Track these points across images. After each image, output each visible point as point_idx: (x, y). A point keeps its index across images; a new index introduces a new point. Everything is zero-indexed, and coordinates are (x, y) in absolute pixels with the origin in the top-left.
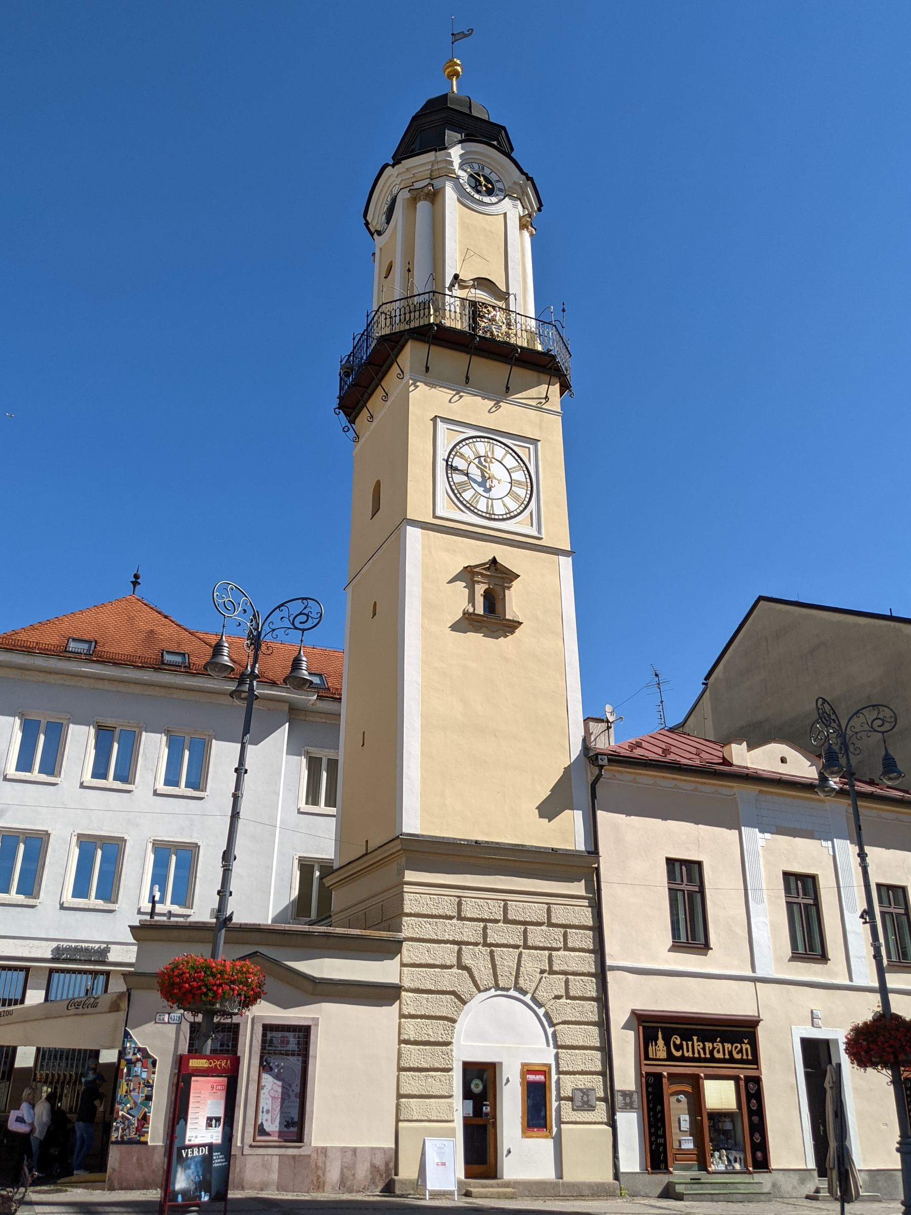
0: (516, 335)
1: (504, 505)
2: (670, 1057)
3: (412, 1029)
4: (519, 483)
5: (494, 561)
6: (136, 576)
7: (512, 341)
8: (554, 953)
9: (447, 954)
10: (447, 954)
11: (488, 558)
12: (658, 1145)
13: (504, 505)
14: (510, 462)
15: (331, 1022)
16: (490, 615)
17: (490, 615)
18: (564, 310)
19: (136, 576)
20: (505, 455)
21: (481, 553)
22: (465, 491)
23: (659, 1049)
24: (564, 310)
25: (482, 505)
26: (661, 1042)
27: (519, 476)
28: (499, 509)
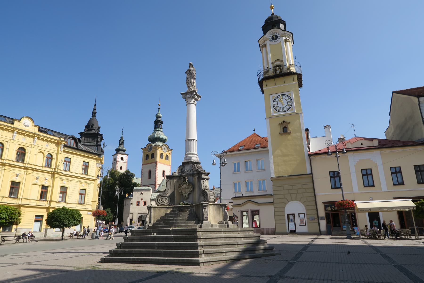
2: (332, 210)
3: (276, 210)
5: (284, 121)
14: (287, 98)
15: (263, 209)
23: (329, 209)
26: (329, 207)
28: (285, 109)
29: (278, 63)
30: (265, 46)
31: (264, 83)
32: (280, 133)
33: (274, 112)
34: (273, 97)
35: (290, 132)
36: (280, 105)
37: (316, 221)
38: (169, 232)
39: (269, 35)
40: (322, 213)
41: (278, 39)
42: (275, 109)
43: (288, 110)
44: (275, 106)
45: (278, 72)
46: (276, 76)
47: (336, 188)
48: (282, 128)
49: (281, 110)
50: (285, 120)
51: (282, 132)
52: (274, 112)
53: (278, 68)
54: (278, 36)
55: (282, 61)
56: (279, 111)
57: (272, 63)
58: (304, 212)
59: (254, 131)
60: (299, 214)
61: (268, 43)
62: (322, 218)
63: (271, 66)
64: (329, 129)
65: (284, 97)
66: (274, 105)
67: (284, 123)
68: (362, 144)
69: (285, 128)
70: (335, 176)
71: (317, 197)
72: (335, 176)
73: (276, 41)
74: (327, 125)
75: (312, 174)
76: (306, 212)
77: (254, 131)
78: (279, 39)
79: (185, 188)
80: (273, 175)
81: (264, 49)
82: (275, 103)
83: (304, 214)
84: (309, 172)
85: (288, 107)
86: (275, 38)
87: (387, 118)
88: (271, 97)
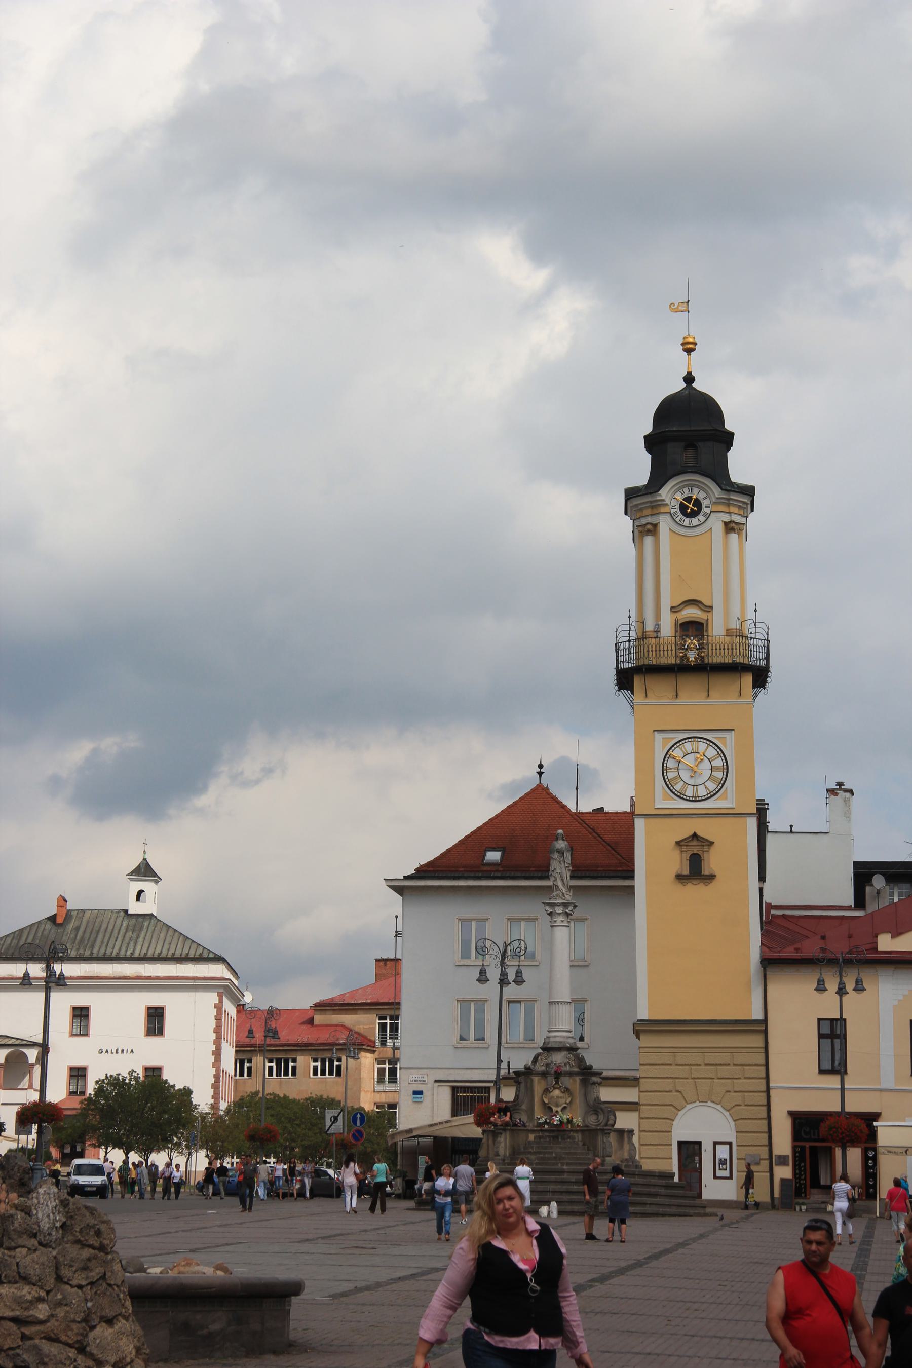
1: (706, 787)
4: (717, 768)
5: (695, 835)
6: (541, 766)
7: (706, 661)
8: (735, 1081)
9: (667, 1084)
10: (667, 1084)
11: (692, 833)
12: (801, 1184)
13: (706, 787)
14: (711, 752)
16: (695, 871)
17: (695, 871)
18: (755, 610)
19: (541, 766)
21: (685, 829)
24: (755, 610)
25: (689, 793)
27: (718, 762)
28: (702, 792)
29: (691, 613)
30: (652, 530)
31: (637, 681)
32: (680, 877)
35: (712, 877)
38: (562, 1172)
40: (783, 1144)
41: (701, 518)
42: (668, 784)
43: (711, 796)
44: (671, 775)
45: (692, 656)
46: (681, 669)
47: (832, 1071)
48: (686, 856)
49: (689, 793)
50: (699, 834)
51: (686, 871)
53: (692, 642)
54: (705, 503)
56: (680, 796)
57: (674, 609)
58: (732, 1139)
59: (540, 774)
60: (715, 1143)
61: (665, 525)
62: (782, 1160)
64: (846, 802)
65: (702, 746)
66: (664, 769)
67: (695, 843)
69: (696, 862)
70: (833, 1033)
71: (772, 1093)
72: (833, 1033)
73: (695, 521)
74: (840, 784)
75: (765, 1021)
77: (540, 774)
78: (708, 516)
79: (558, 1097)
80: (643, 1013)
81: (649, 540)
82: (671, 764)
83: (730, 1144)
84: (758, 1015)
85: (712, 786)
88: (658, 737)
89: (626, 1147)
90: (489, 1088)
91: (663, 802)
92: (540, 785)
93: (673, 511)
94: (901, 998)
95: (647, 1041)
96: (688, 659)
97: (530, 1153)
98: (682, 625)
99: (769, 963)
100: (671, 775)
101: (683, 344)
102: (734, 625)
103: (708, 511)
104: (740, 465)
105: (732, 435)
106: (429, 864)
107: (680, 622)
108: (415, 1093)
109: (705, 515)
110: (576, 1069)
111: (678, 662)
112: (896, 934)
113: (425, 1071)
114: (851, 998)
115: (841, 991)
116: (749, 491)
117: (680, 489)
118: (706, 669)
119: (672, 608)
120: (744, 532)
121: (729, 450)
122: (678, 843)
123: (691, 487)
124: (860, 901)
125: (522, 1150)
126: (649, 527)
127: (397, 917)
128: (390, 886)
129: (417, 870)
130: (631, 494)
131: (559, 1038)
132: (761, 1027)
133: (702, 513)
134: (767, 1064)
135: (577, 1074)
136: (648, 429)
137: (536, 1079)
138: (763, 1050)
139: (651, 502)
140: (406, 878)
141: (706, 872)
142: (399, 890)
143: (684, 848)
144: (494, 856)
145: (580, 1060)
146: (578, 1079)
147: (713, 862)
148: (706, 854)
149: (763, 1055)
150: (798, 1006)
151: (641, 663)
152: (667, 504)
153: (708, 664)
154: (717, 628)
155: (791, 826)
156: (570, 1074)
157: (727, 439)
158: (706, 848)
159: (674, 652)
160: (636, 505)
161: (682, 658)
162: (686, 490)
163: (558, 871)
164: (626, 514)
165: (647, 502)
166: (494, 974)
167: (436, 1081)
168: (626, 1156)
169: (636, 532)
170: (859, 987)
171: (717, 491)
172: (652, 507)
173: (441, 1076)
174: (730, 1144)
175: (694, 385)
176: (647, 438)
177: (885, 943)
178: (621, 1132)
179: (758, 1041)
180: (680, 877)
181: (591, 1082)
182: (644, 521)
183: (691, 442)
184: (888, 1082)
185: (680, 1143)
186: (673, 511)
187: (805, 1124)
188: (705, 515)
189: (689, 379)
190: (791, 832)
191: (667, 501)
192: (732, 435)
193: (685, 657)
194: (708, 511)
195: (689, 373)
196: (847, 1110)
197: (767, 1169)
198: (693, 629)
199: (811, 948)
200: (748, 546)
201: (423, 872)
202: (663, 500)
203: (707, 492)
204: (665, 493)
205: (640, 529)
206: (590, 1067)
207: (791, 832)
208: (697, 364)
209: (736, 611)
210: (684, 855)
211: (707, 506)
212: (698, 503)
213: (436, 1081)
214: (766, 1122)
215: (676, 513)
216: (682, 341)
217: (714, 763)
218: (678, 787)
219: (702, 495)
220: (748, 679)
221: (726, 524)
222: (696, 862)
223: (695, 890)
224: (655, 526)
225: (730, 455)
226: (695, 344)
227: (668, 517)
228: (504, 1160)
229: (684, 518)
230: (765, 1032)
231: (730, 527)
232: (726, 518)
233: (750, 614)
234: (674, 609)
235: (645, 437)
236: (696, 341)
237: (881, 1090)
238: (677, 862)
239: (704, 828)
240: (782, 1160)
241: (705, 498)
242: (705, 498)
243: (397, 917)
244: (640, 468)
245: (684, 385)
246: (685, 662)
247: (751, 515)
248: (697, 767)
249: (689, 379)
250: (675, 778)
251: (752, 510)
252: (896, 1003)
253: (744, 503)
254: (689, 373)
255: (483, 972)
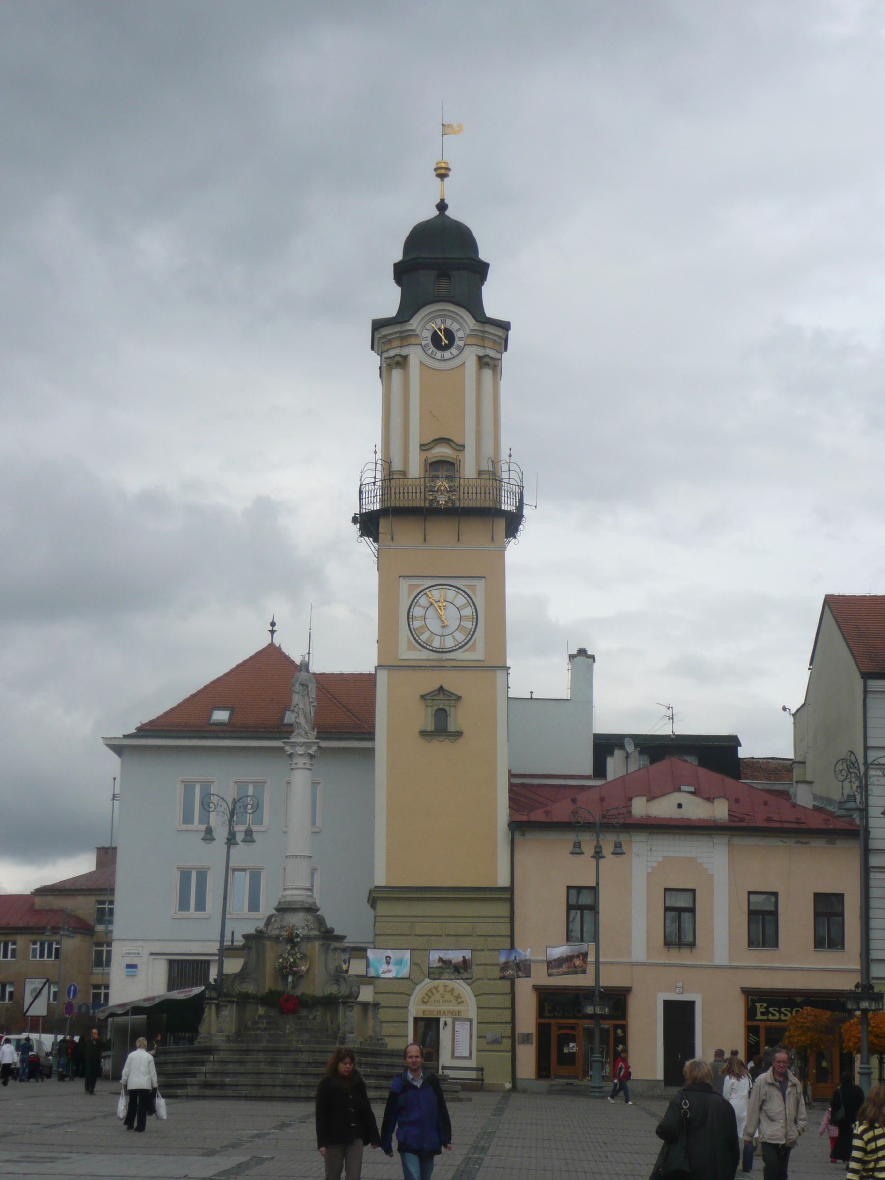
0: (459, 499)
1: (454, 638)
4: (467, 618)
5: (441, 689)
6: (273, 624)
7: (457, 505)
11: (437, 687)
13: (454, 638)
14: (461, 600)
17: (441, 728)
19: (273, 624)
20: (456, 596)
21: (430, 682)
22: (422, 633)
28: (450, 643)
30: (401, 362)
32: (424, 733)
33: (410, 648)
34: (411, 587)
35: (458, 734)
36: (434, 625)
37: (507, 1043)
39: (423, 324)
40: (527, 1020)
41: (454, 351)
44: (417, 624)
48: (430, 711)
49: (436, 643)
50: (446, 687)
51: (430, 727)
52: (410, 648)
53: (442, 484)
54: (458, 335)
55: (461, 448)
56: (425, 647)
59: (272, 632)
61: (415, 356)
62: (526, 1039)
63: (415, 470)
65: (451, 594)
66: (409, 617)
67: (441, 696)
68: (680, 806)
69: (441, 715)
70: (583, 905)
72: (583, 905)
73: (447, 354)
75: (511, 889)
76: (478, 1015)
77: (272, 632)
78: (461, 350)
80: (381, 880)
81: (397, 373)
83: (470, 1021)
84: (503, 881)
85: (460, 637)
86: (442, 342)
87: (804, 676)
88: (404, 584)
89: (371, 1022)
90: (208, 962)
91: (407, 653)
92: (272, 645)
93: (424, 343)
94: (655, 865)
95: (383, 908)
96: (438, 502)
97: (258, 1029)
98: (431, 464)
99: (518, 827)
100: (417, 624)
101: (436, 169)
102: (486, 466)
103: (461, 343)
104: (495, 300)
105: (485, 266)
106: (151, 723)
107: (429, 461)
108: (129, 966)
109: (458, 347)
110: (316, 933)
111: (427, 505)
112: (651, 798)
113: (140, 942)
114: (609, 861)
115: (598, 855)
116: (505, 326)
117: (432, 319)
118: (456, 513)
119: (421, 445)
120: (498, 368)
121: (482, 283)
122: (423, 697)
123: (444, 317)
124: (600, 770)
125: (250, 1024)
126: (398, 359)
127: (114, 779)
128: (109, 746)
129: (139, 729)
130: (378, 325)
131: (296, 895)
132: (507, 895)
133: (455, 345)
134: (512, 936)
135: (316, 938)
136: (398, 256)
137: (268, 943)
138: (508, 920)
139: (401, 332)
140: (126, 736)
141: (452, 728)
142: (118, 749)
143: (429, 703)
144: (221, 716)
145: (321, 921)
146: (317, 944)
147: (458, 719)
148: (453, 710)
149: (509, 925)
150: (548, 873)
151: (386, 505)
152: (417, 336)
153: (459, 507)
154: (469, 470)
155: (532, 693)
156: (308, 938)
157: (481, 270)
158: (453, 703)
159: (423, 494)
160: (385, 336)
161: (431, 501)
162: (438, 321)
163: (301, 706)
164: (372, 348)
165: (396, 333)
166: (221, 834)
167: (152, 954)
168: (370, 1033)
169: (384, 365)
170: (618, 851)
171: (471, 322)
172: (402, 339)
173: (157, 947)
174: (470, 1021)
175: (448, 213)
176: (397, 266)
177: (640, 807)
178: (365, 1005)
179: (502, 910)
180: (424, 733)
181: (332, 947)
182: (393, 353)
183: (443, 270)
184: (639, 954)
185: (416, 1020)
186: (424, 343)
187: (550, 1001)
188: (458, 347)
189: (442, 206)
190: (532, 698)
191: (418, 332)
192: (485, 266)
193: (435, 500)
194: (461, 343)
195: (442, 200)
196: (602, 984)
197: (509, 1048)
198: (441, 467)
199: (561, 811)
200: (503, 384)
201: (144, 731)
202: (414, 331)
203: (463, 325)
204: (415, 323)
205: (389, 361)
206: (331, 931)
207: (532, 698)
208: (452, 191)
209: (488, 449)
210: (429, 710)
211: (461, 339)
212: (449, 334)
213: (152, 954)
214: (509, 998)
215: (427, 345)
216: (435, 166)
217: (463, 613)
218: (424, 637)
219: (454, 327)
220: (501, 525)
221: (480, 358)
222: (441, 715)
223: (440, 748)
224: (405, 358)
225: (484, 288)
226: (449, 169)
227: (419, 349)
228: (228, 1037)
229: (436, 350)
230: (511, 901)
231: (484, 362)
232: (481, 352)
233: (504, 455)
234: (424, 447)
235: (395, 265)
236: (450, 166)
237: (633, 964)
238: (424, 719)
239: (452, 682)
240: (526, 1039)
241: (458, 330)
242: (458, 330)
243: (114, 779)
244: (388, 299)
245: (436, 213)
246: (435, 505)
247: (505, 354)
248: (445, 617)
249: (442, 206)
250: (422, 627)
251: (506, 349)
252: (650, 870)
253: (499, 337)
254: (442, 200)
255: (209, 831)
